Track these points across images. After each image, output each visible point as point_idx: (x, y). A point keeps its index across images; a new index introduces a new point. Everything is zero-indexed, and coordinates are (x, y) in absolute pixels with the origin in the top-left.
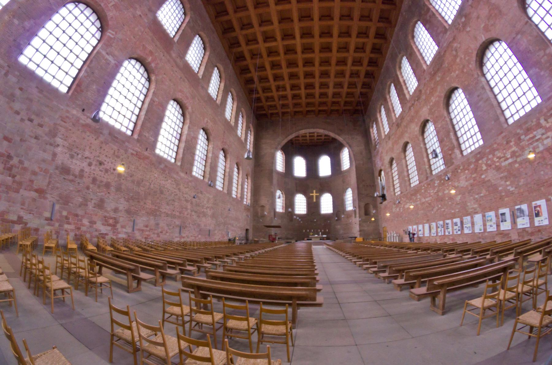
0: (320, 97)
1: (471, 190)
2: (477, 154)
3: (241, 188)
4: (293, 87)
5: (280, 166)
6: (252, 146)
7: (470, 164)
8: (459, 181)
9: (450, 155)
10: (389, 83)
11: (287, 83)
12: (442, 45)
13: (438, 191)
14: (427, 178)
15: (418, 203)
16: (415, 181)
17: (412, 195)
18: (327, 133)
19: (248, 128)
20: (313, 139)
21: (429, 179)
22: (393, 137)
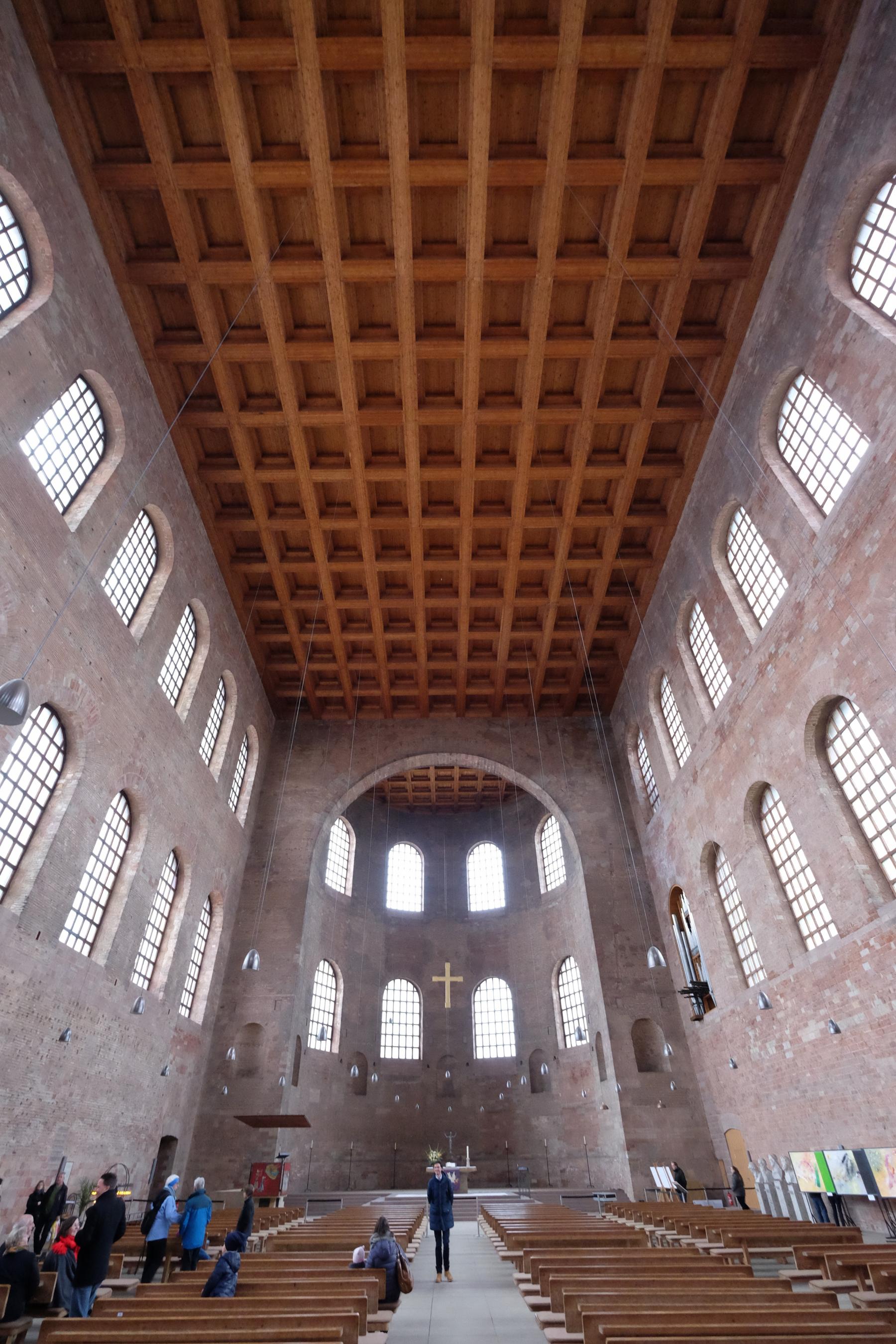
0: (470, 657)
3: (178, 950)
4: (393, 620)
6: (246, 797)
10: (684, 605)
14: (874, 914)
16: (820, 925)
17: (819, 984)
19: (239, 732)
20: (450, 789)
22: (707, 771)
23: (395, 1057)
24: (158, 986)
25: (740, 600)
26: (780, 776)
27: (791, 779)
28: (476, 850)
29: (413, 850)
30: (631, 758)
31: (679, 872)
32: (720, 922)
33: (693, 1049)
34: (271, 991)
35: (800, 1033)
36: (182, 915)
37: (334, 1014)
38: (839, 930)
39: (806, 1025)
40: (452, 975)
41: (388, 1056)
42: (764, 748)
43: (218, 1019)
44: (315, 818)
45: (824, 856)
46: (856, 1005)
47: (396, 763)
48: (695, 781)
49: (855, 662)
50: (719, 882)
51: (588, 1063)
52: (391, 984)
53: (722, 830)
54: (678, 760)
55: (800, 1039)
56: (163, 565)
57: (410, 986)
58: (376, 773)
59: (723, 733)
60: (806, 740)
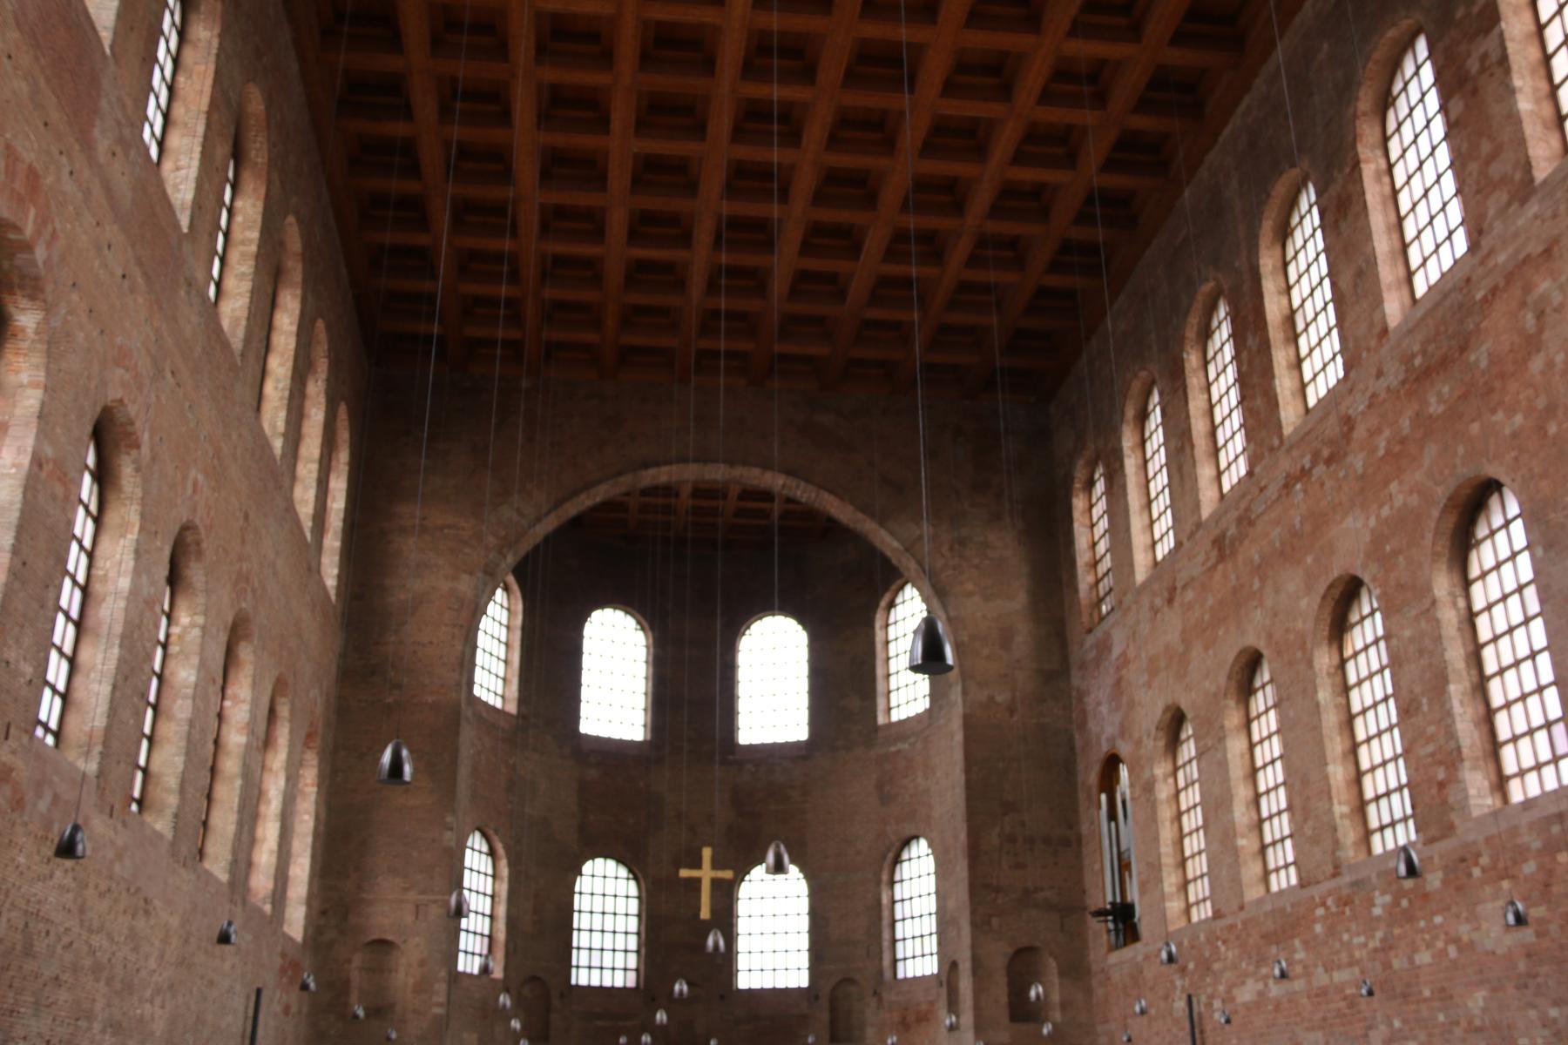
2: (1548, 821)
4: (643, 226)
5: (493, 676)
7: (1521, 853)
8: (1473, 918)
11: (618, 204)
12: (1491, 252)
13: (1387, 947)
15: (1299, 985)
17: (1268, 938)
18: (805, 493)
21: (1346, 879)
23: (595, 982)
24: (261, 896)
26: (1279, 653)
27: (1291, 663)
30: (1079, 503)
32: (1168, 824)
34: (406, 889)
35: (1235, 992)
36: (282, 782)
37: (492, 917)
38: (1300, 878)
39: (1243, 983)
41: (583, 981)
42: (1269, 603)
44: (465, 585)
45: (1305, 782)
46: (1299, 969)
47: (622, 479)
48: (1170, 601)
49: (1388, 548)
50: (1180, 762)
51: (932, 1003)
52: (587, 867)
53: (1193, 694)
54: (1154, 543)
55: (1233, 1000)
57: (623, 872)
58: (583, 497)
59: (1223, 548)
60: (1317, 620)
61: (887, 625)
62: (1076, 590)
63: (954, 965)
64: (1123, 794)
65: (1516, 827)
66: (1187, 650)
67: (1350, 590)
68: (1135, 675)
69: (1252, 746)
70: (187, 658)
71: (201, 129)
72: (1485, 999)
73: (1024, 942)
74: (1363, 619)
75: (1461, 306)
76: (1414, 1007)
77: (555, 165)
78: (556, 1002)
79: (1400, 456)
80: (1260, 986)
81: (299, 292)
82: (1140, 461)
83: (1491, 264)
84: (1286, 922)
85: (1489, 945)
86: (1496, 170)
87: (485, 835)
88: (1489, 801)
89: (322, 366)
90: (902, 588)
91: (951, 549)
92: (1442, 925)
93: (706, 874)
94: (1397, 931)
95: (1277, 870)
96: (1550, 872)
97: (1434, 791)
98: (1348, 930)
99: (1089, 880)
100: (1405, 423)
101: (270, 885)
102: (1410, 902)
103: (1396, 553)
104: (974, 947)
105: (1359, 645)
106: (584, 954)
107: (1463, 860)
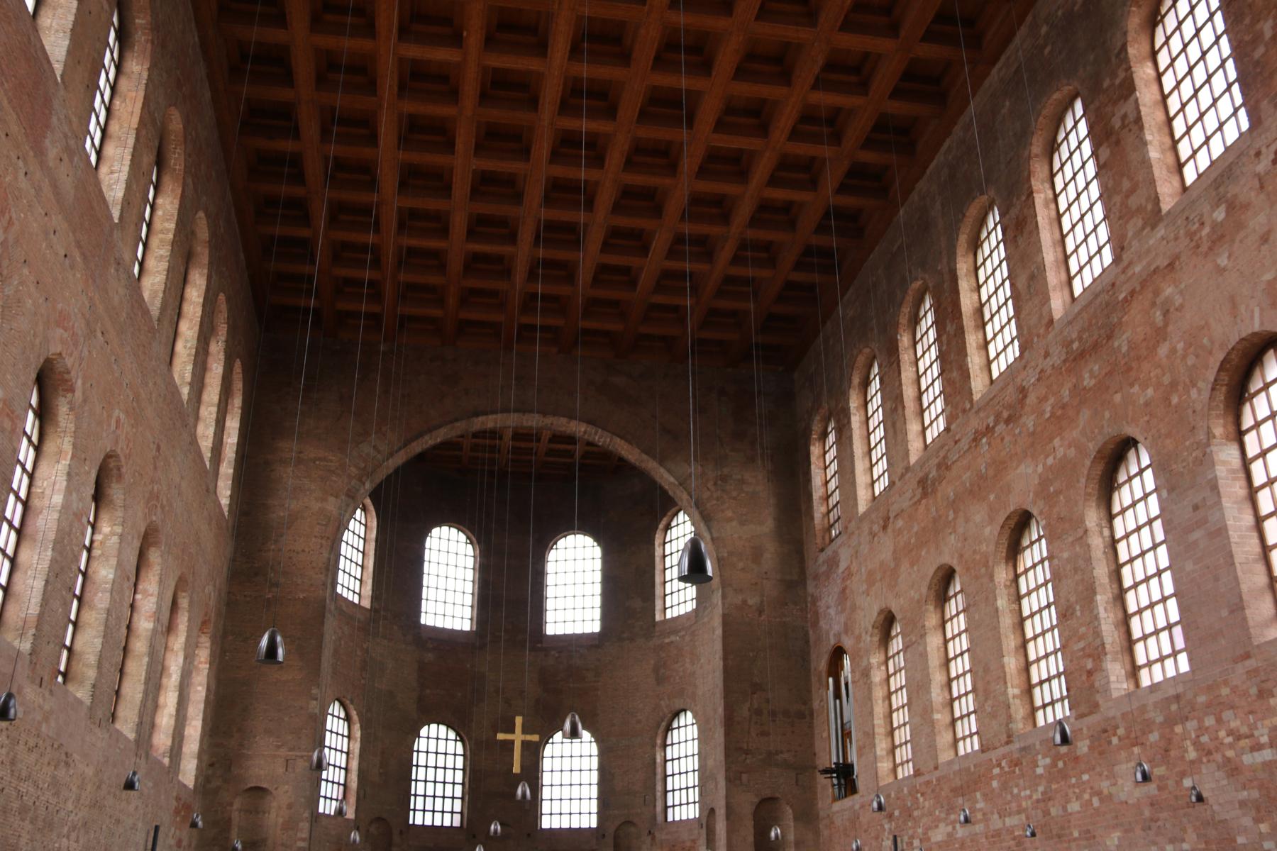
1: (1152, 820)
2: (1168, 700)
4: (479, 226)
5: (353, 578)
7: (1148, 726)
8: (1112, 776)
9: (1090, 673)
13: (1047, 798)
15: (979, 828)
17: (957, 791)
18: (602, 438)
21: (1016, 746)
23: (428, 822)
24: (161, 751)
25: (977, 327)
26: (968, 569)
27: (977, 578)
28: (561, 543)
29: (462, 537)
30: (815, 450)
31: (846, 632)
32: (880, 702)
33: (826, 833)
34: (279, 747)
36: (181, 660)
38: (981, 745)
39: (937, 827)
40: (524, 731)
41: (419, 821)
42: (961, 530)
43: (208, 780)
44: (332, 505)
45: (987, 670)
46: (979, 816)
47: (457, 424)
48: (885, 528)
50: (891, 654)
51: (694, 841)
52: (424, 732)
54: (873, 482)
55: (929, 839)
56: (167, 179)
57: (452, 735)
58: (427, 437)
59: (926, 487)
60: (997, 543)
61: (665, 543)
62: (812, 518)
63: (712, 811)
64: (846, 678)
65: (1144, 706)
66: (897, 566)
67: (1022, 521)
68: (857, 585)
69: (946, 642)
70: (107, 560)
71: (131, 142)
72: (1119, 838)
73: (767, 793)
74: (1032, 543)
75: (1107, 304)
76: (1066, 845)
77: (411, 177)
78: (396, 838)
79: (1061, 418)
80: (950, 828)
81: (206, 271)
82: (863, 418)
83: (1130, 273)
84: (970, 780)
85: (1123, 797)
86: (1134, 202)
87: (342, 704)
88: (1125, 686)
89: (223, 330)
90: (676, 514)
91: (715, 484)
92: (1088, 781)
93: (518, 737)
94: (1054, 787)
95: (964, 738)
96: (1169, 741)
97: (1084, 678)
98: (1017, 786)
99: (818, 745)
100: (1066, 393)
101: (169, 743)
102: (1065, 763)
103: (1058, 493)
104: (728, 797)
105: (1029, 564)
106: (420, 800)
107: (1105, 731)
